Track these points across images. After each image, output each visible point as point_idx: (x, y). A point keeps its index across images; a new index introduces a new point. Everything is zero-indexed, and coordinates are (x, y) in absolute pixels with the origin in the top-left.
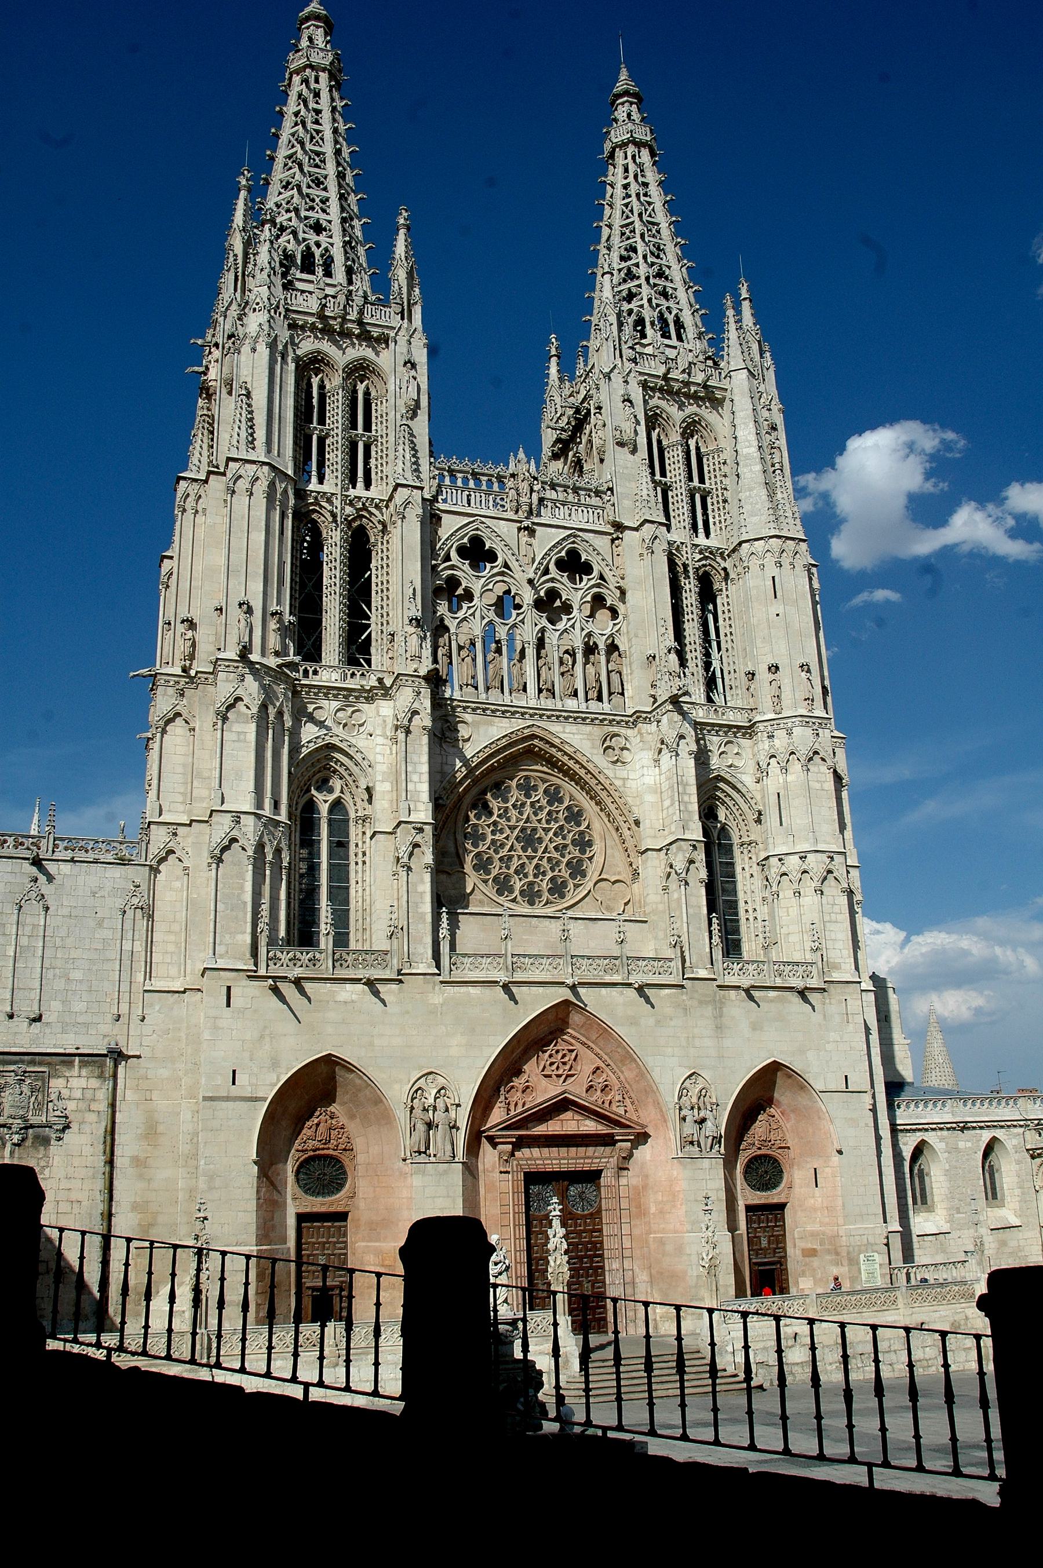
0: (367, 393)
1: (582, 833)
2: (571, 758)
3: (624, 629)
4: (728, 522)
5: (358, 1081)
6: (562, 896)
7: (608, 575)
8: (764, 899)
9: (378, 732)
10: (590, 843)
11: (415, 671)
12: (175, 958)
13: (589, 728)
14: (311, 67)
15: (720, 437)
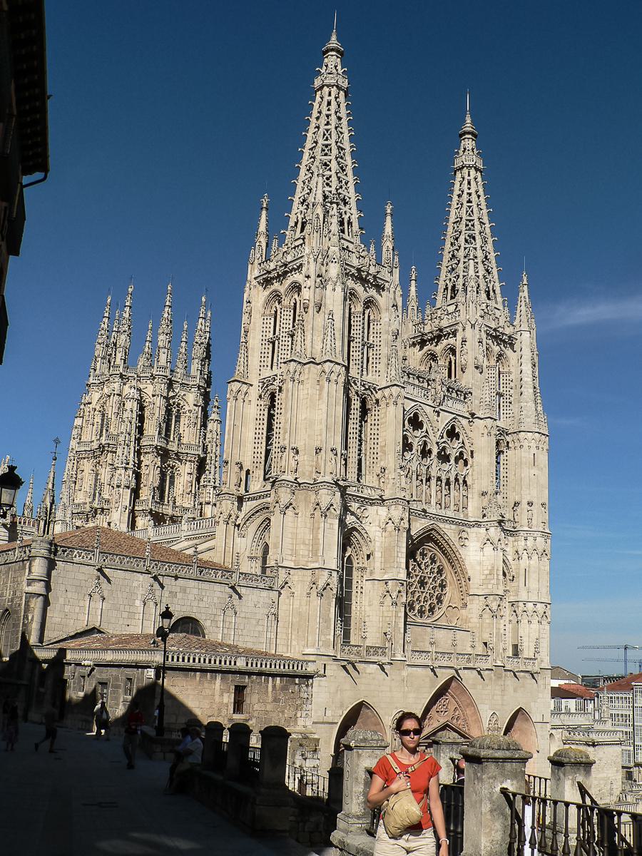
0: (369, 316)
1: (442, 580)
2: (446, 542)
3: (470, 473)
4: (511, 415)
5: (370, 714)
6: (433, 614)
7: (466, 442)
8: (510, 621)
9: (377, 524)
10: (445, 586)
11: (404, 497)
12: (286, 642)
13: (453, 527)
14: (337, 87)
15: (511, 365)
